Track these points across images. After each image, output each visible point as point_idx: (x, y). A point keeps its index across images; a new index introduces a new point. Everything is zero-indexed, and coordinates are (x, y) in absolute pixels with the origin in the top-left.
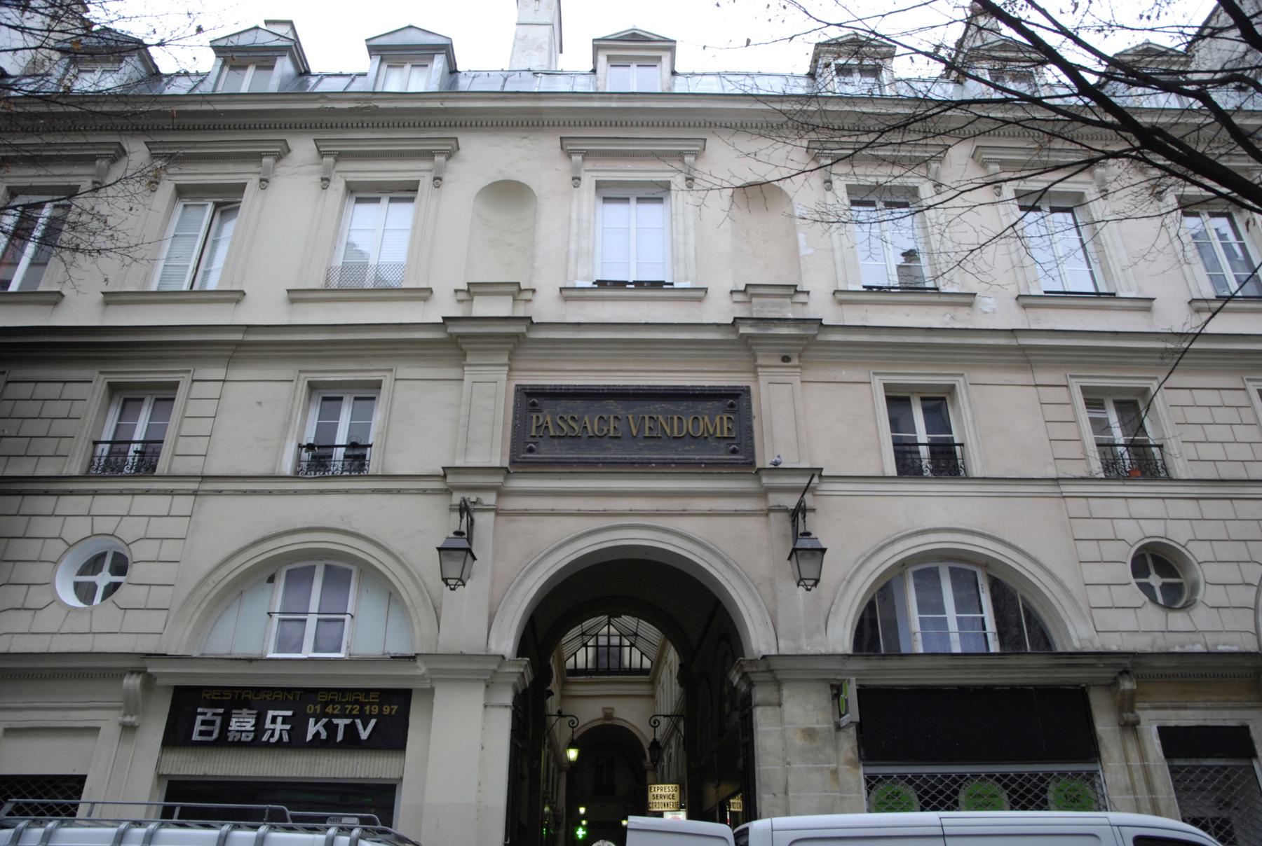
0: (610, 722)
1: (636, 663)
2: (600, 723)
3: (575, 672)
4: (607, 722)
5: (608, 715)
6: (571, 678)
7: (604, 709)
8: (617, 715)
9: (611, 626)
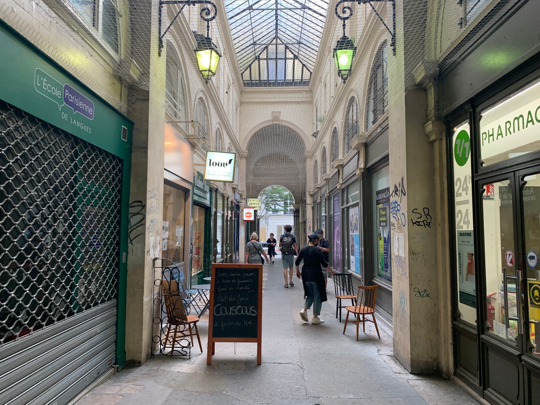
2: (270, 123)
4: (275, 123)
5: (276, 118)
7: (273, 112)
9: (278, 39)
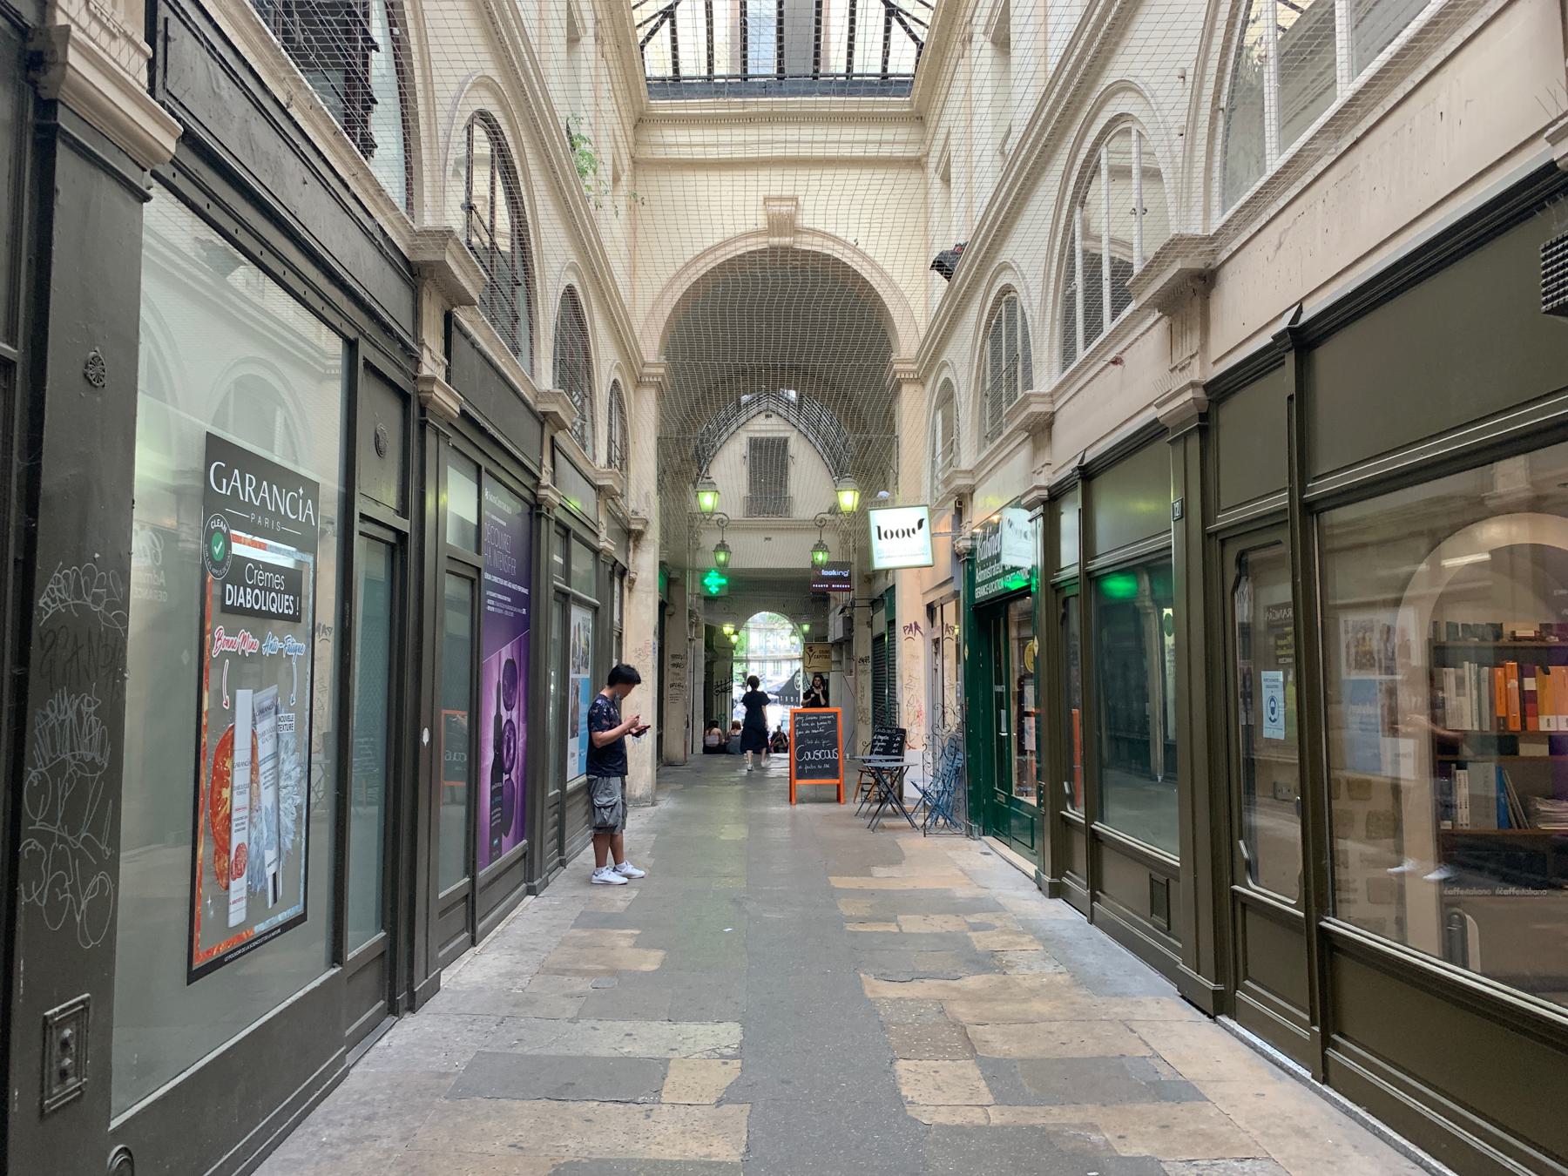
0: (786, 241)
1: (868, 62)
3: (675, 84)
4: (775, 241)
5: (782, 224)
6: (662, 106)
7: (766, 199)
8: (805, 221)
